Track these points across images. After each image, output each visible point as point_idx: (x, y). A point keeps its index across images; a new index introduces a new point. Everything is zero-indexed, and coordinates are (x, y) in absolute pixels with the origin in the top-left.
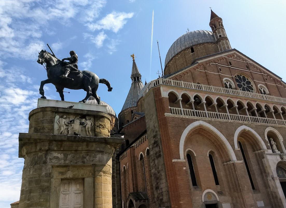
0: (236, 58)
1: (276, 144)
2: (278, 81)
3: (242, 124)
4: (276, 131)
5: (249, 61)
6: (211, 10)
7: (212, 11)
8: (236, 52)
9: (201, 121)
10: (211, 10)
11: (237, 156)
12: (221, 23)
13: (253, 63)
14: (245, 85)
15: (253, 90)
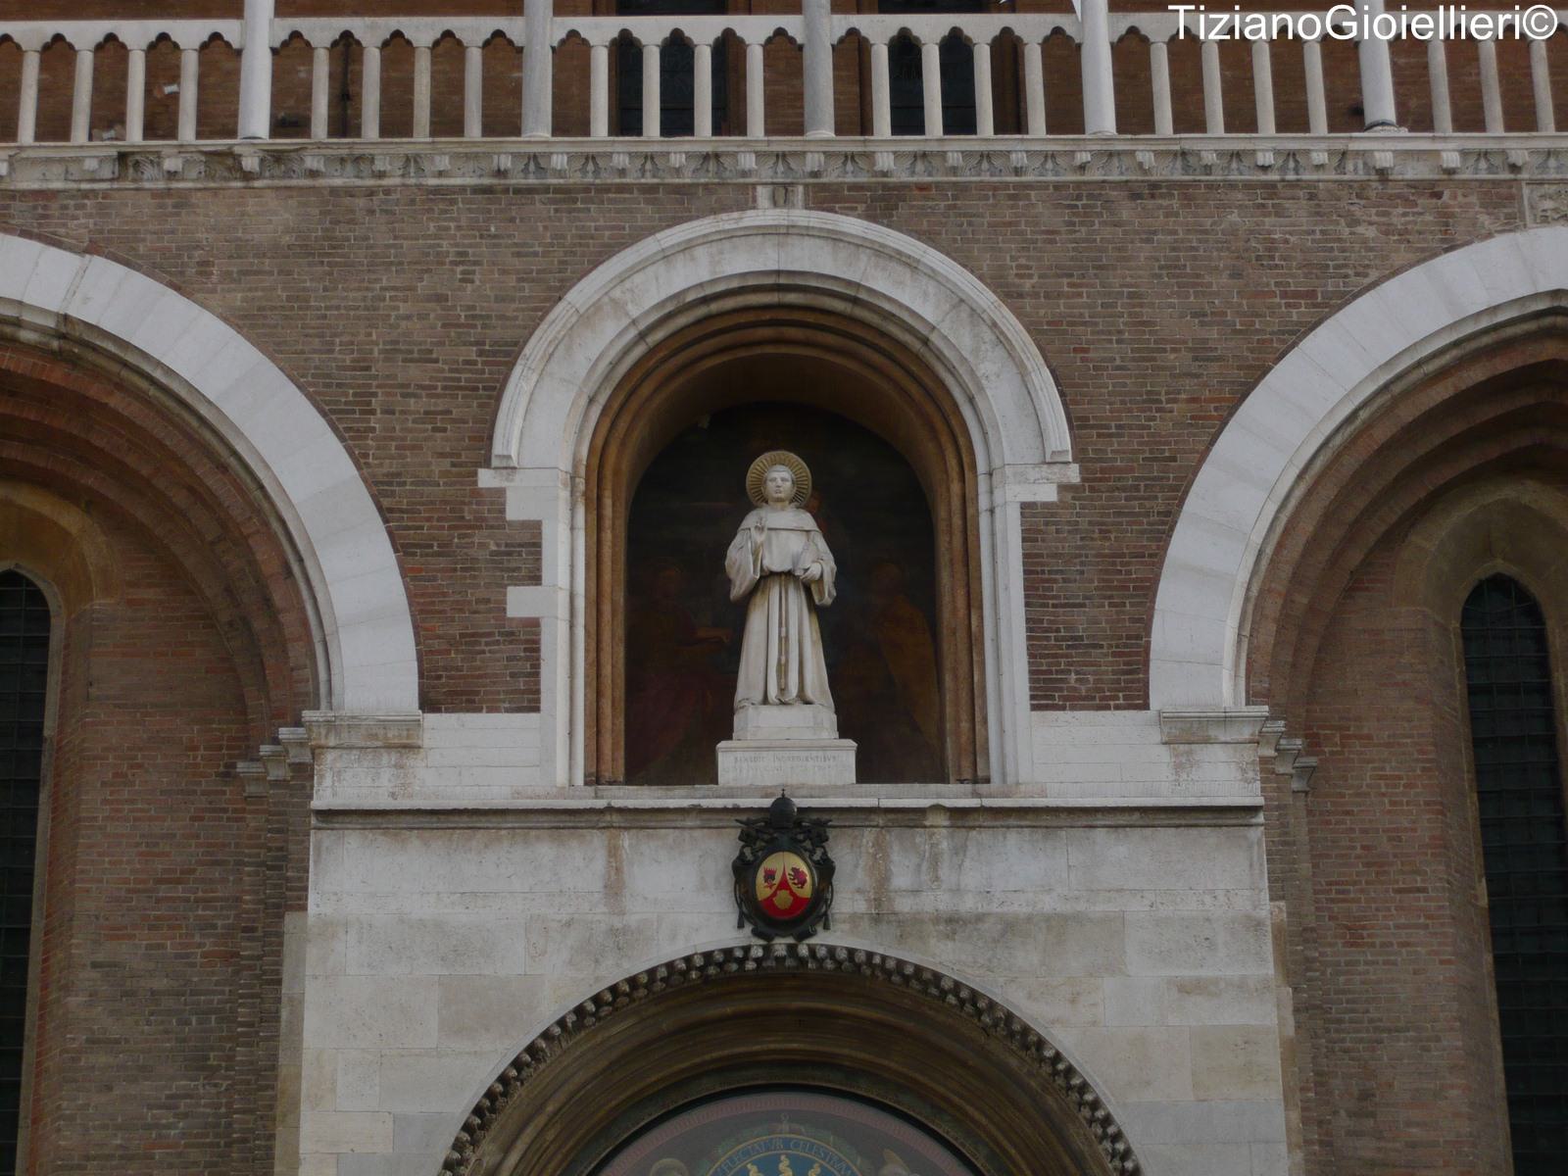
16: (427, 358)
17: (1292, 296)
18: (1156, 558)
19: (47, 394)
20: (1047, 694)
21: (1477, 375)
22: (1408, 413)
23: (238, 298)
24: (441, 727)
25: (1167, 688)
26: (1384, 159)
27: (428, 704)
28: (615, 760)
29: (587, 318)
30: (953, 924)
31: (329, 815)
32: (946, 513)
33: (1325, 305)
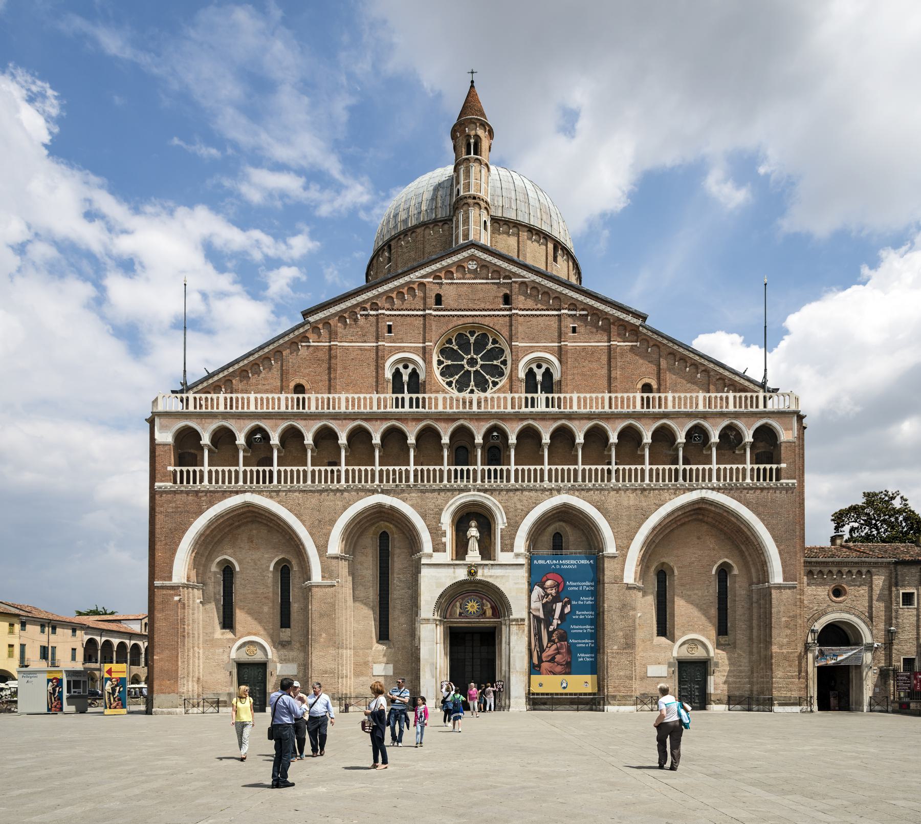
0: (475, 274)
1: (478, 535)
2: (623, 325)
3: (373, 492)
4: (490, 501)
5: (523, 277)
6: (472, 82)
7: (472, 86)
8: (476, 252)
9: (248, 494)
10: (472, 82)
11: (323, 570)
12: (472, 141)
13: (538, 279)
14: (472, 362)
15: (501, 374)
16: (433, 510)
17: (533, 503)
18: (515, 535)
19: (388, 514)
20: (502, 550)
21: (555, 512)
22: (546, 517)
23: (410, 503)
24: (435, 554)
25: (516, 550)
26: (545, 486)
27: (434, 551)
28: (454, 558)
29: (451, 505)
30: (491, 576)
31: (423, 564)
32: (493, 527)
33: (536, 504)
